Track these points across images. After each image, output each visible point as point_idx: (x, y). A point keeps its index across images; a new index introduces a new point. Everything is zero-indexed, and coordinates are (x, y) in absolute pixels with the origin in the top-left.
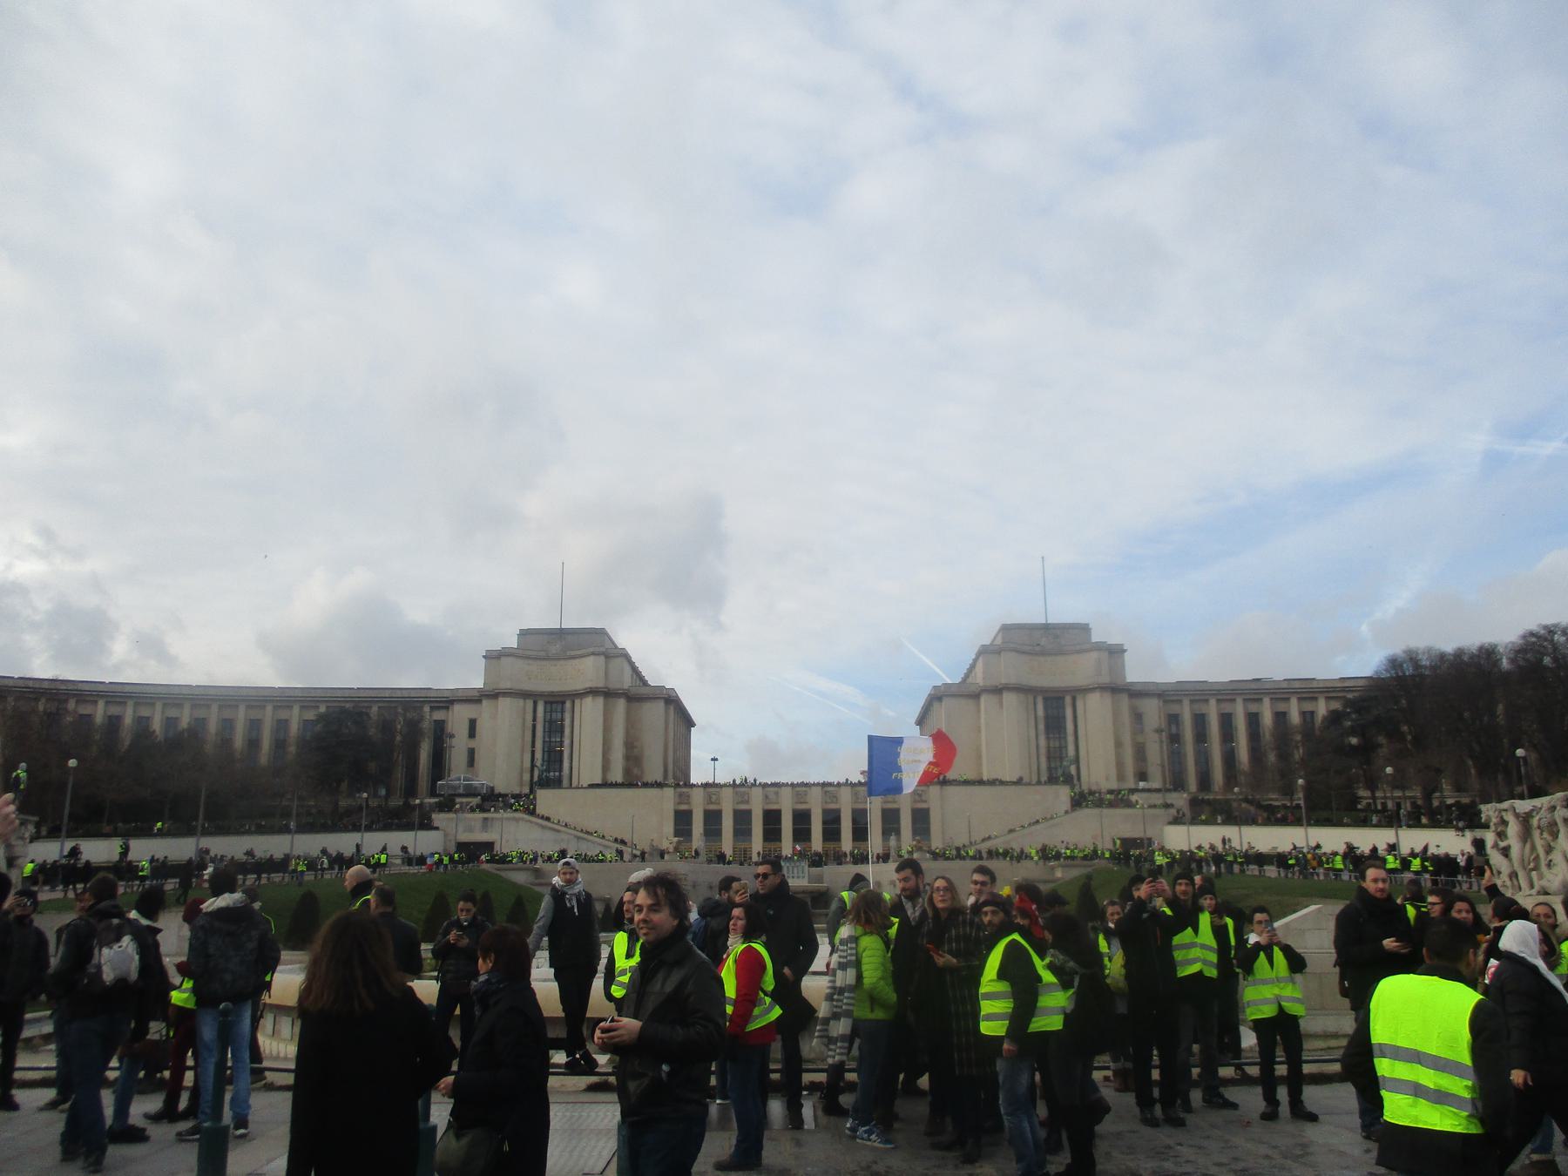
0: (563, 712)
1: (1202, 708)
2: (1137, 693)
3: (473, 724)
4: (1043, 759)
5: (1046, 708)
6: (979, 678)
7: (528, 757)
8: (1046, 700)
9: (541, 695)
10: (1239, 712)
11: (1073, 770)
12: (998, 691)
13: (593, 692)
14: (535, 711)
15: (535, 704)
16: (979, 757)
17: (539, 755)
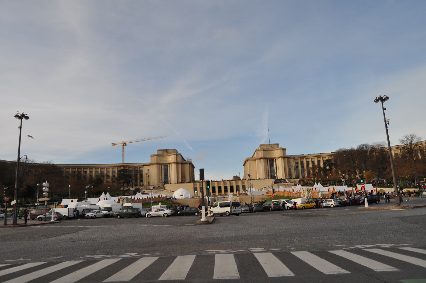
2: (289, 158)
3: (148, 170)
4: (270, 173)
5: (270, 162)
6: (255, 156)
7: (161, 177)
9: (163, 164)
10: (310, 161)
11: (276, 175)
12: (260, 159)
13: (174, 163)
16: (256, 173)
17: (163, 176)
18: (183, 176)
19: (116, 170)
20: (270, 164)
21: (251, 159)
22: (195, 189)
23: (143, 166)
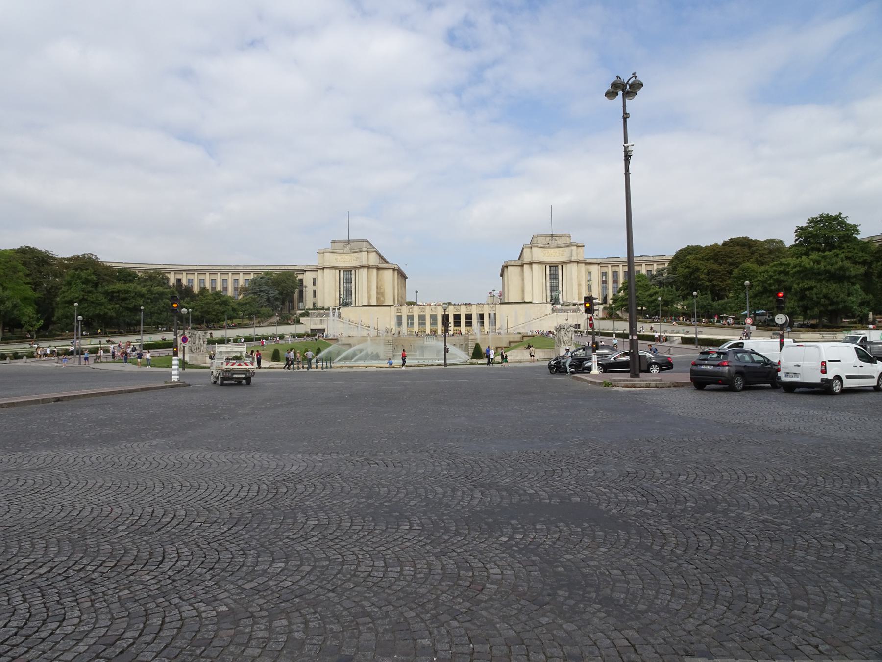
1: (616, 269)
3: (314, 279)
4: (548, 292)
12: (531, 264)
16: (523, 291)
18: (380, 293)
21: (513, 263)
22: (400, 318)
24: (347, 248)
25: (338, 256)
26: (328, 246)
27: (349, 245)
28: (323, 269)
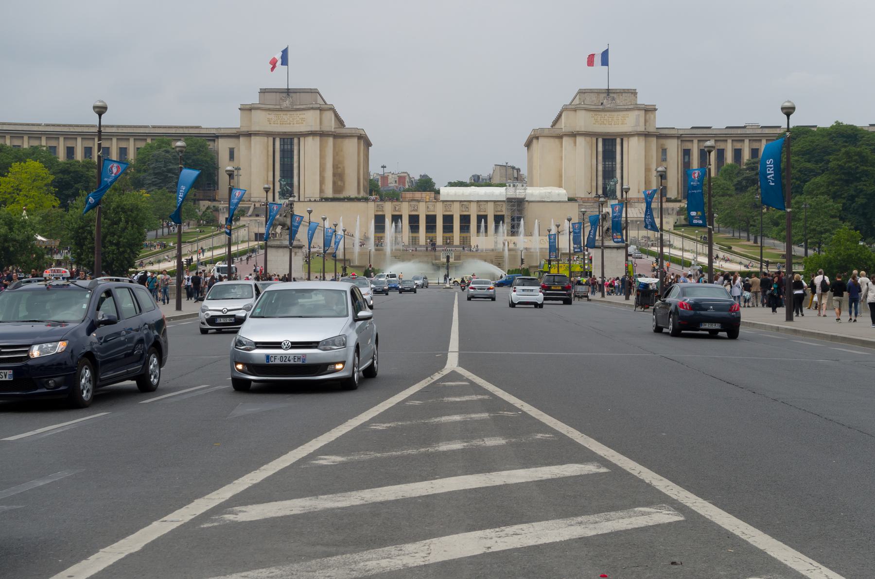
0: (292, 144)
2: (661, 136)
4: (600, 179)
8: (604, 140)
13: (312, 134)
14: (274, 144)
15: (274, 139)
16: (561, 176)
18: (339, 176)
19: (132, 147)
20: (604, 152)
21: (546, 133)
22: (380, 221)
23: (214, 137)
24: (287, 104)
25: (272, 116)
26: (255, 99)
27: (287, 98)
28: (249, 135)
